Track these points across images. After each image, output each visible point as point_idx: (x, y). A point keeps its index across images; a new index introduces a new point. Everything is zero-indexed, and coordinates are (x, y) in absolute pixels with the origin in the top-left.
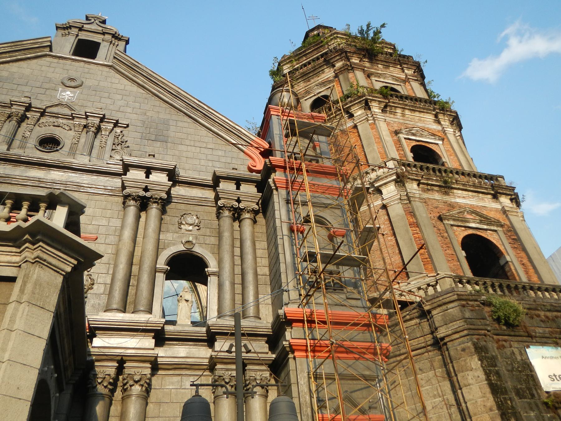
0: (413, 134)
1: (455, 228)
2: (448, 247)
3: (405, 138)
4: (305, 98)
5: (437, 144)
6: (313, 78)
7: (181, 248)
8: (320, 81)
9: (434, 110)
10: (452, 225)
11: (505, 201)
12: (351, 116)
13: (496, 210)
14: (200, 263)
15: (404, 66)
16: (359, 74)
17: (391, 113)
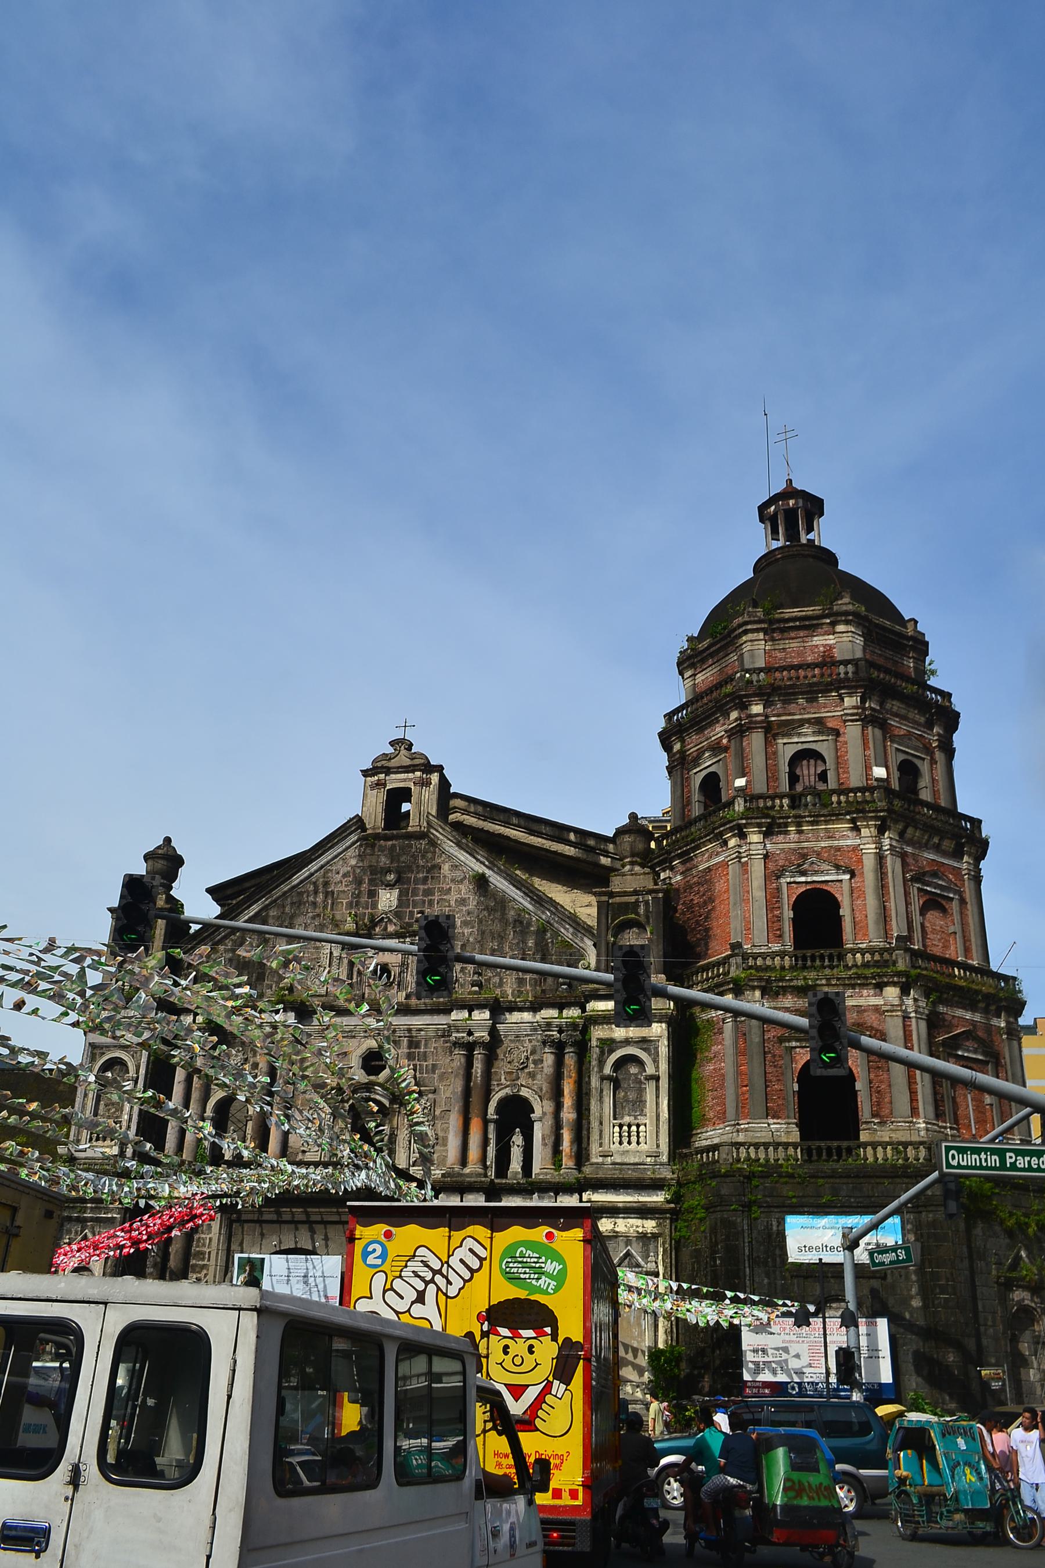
0: (803, 873)
1: (798, 1049)
2: (779, 1080)
3: (788, 883)
4: (695, 771)
5: (841, 881)
6: (706, 728)
7: (508, 1091)
8: (713, 739)
9: (848, 813)
10: (796, 1047)
11: (892, 993)
12: (725, 843)
13: (877, 1009)
14: (526, 1107)
15: (843, 691)
16: (756, 740)
17: (780, 833)
